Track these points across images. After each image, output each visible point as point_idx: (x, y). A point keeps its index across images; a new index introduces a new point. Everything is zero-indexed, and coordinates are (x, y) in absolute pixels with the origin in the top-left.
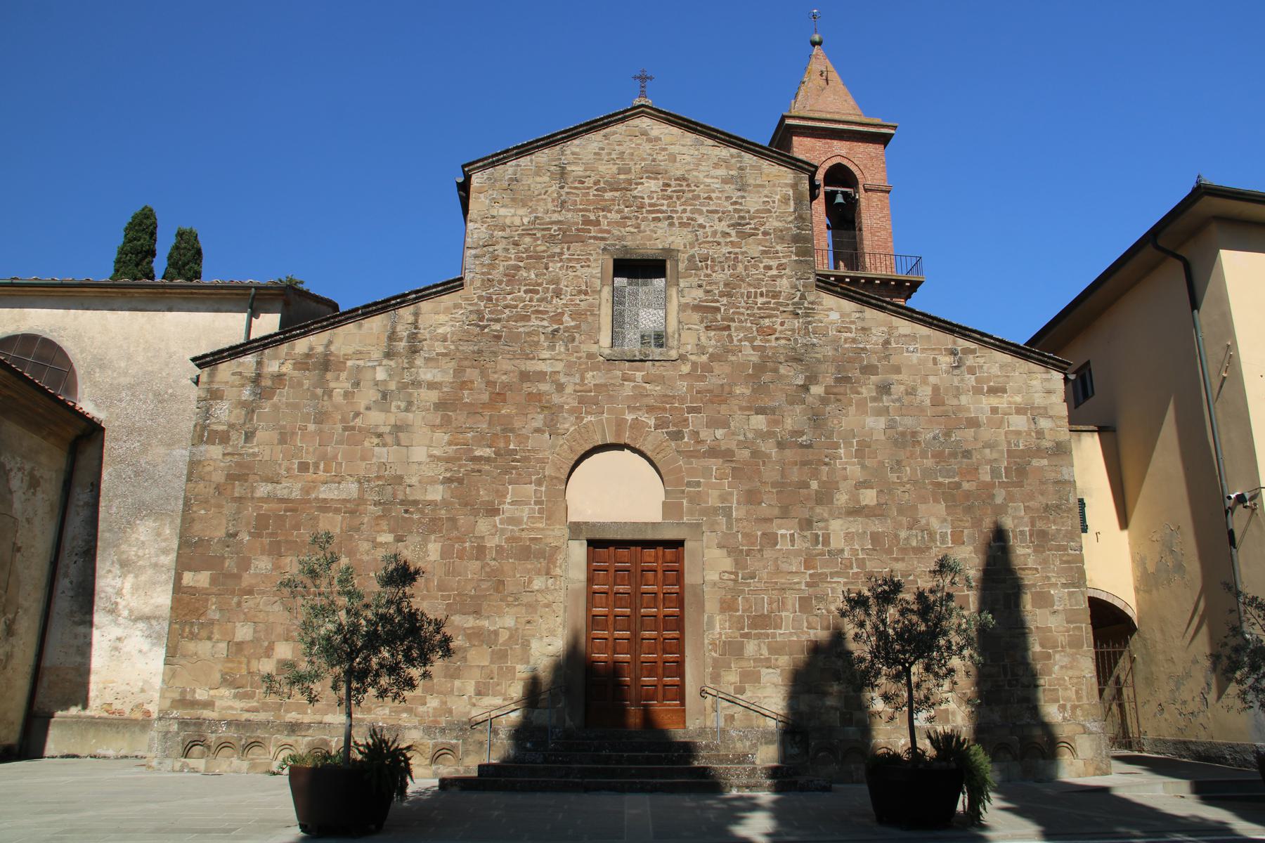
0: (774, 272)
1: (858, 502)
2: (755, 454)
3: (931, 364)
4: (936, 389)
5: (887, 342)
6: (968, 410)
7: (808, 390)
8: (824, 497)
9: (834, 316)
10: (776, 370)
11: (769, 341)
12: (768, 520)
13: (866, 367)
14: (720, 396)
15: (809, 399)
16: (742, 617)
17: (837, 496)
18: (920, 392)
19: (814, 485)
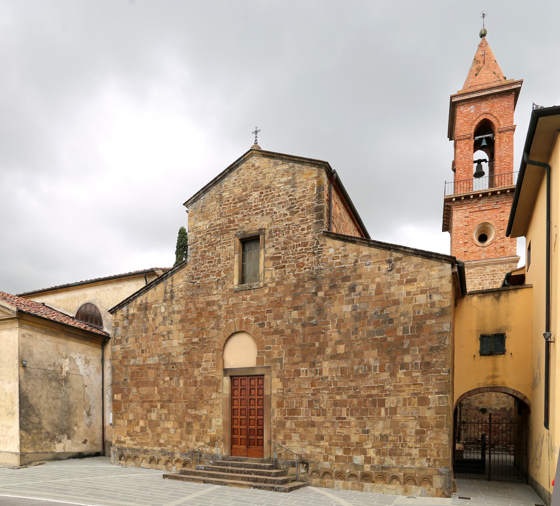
0: (306, 232)
1: (336, 352)
2: (293, 331)
3: (377, 271)
4: (378, 285)
5: (356, 261)
6: (394, 295)
7: (317, 294)
8: (321, 351)
9: (332, 251)
10: (303, 286)
11: (301, 271)
12: (297, 363)
13: (345, 277)
14: (279, 303)
15: (318, 300)
16: (285, 410)
17: (327, 349)
18: (370, 288)
19: (317, 344)
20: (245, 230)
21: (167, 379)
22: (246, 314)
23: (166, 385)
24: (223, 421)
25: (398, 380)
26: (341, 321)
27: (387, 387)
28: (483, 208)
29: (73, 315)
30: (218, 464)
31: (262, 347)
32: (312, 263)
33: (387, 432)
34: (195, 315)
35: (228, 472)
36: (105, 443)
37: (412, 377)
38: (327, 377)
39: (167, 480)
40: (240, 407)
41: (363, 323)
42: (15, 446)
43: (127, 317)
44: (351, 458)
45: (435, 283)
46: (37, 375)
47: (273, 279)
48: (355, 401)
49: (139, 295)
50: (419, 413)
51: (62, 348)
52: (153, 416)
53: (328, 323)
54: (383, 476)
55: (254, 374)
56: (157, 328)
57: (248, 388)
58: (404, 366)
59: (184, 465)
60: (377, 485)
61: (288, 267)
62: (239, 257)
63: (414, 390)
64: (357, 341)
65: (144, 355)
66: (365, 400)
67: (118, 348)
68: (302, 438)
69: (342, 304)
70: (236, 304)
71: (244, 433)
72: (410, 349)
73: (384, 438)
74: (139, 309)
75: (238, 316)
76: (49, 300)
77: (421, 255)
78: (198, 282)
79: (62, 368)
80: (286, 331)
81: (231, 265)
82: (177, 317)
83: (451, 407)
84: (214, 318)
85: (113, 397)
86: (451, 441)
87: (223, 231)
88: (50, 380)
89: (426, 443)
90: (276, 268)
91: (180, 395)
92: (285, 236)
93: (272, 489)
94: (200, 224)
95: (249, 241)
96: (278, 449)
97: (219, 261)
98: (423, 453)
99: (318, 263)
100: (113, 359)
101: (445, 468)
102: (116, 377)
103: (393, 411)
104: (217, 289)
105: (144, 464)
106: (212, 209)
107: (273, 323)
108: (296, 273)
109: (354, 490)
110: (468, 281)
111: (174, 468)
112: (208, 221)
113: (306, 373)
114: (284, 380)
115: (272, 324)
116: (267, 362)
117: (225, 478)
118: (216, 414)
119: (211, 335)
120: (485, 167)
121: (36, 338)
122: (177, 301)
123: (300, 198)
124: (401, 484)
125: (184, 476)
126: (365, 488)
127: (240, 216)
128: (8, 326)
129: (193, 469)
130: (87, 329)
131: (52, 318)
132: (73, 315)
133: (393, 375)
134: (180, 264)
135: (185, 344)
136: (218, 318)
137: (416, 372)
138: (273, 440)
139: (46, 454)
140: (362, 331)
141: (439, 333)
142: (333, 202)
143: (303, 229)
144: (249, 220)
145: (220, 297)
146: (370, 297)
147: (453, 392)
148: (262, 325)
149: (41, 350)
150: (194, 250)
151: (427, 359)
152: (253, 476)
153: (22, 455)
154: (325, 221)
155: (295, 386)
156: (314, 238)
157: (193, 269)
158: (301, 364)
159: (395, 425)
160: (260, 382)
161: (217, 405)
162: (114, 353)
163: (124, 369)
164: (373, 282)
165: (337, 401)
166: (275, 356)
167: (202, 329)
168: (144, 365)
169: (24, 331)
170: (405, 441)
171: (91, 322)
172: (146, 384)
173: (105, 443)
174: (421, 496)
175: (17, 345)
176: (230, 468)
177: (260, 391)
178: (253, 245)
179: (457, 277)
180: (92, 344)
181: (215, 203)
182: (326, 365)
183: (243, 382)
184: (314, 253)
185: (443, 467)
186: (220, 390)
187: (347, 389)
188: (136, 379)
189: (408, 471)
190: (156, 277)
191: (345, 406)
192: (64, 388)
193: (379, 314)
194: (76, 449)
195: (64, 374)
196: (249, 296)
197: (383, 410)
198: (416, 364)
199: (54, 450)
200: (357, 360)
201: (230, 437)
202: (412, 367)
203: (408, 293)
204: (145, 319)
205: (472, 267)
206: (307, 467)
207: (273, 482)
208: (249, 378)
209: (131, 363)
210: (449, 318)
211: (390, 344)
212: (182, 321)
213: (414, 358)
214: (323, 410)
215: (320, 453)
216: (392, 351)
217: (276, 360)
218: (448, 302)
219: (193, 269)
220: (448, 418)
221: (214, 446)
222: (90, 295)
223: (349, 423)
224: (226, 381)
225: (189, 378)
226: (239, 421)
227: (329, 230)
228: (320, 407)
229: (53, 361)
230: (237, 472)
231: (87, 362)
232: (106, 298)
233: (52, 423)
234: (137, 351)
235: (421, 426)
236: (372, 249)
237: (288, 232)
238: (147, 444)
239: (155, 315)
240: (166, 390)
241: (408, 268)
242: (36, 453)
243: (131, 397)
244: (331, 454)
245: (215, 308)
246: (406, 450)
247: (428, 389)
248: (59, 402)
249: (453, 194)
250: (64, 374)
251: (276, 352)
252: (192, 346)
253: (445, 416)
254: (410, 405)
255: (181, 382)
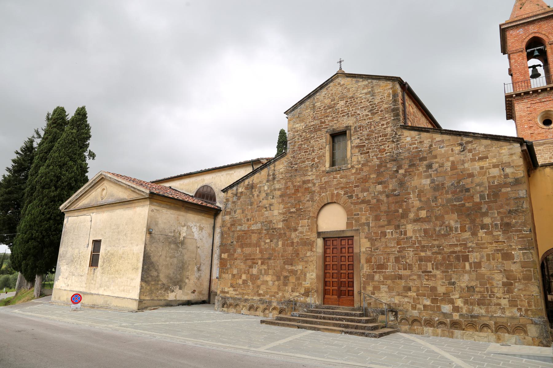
0: (385, 126)
1: (418, 216)
2: (378, 200)
3: (450, 152)
4: (453, 162)
5: (431, 146)
7: (398, 172)
8: (404, 215)
9: (409, 139)
10: (386, 166)
14: (365, 180)
15: (399, 176)
16: (373, 265)
17: (410, 214)
19: (400, 211)
20: (335, 127)
21: (268, 241)
22: (336, 189)
23: (267, 246)
24: (317, 276)
25: (480, 239)
26: (421, 192)
27: (470, 245)
28: (543, 100)
29: (193, 194)
30: (312, 312)
31: (352, 214)
32: (392, 148)
33: (473, 284)
34: (293, 191)
35: (320, 319)
36: (210, 293)
37: (493, 236)
38: (412, 237)
39: (264, 325)
40: (332, 263)
41: (442, 193)
42: (135, 294)
43: (236, 195)
44: (439, 308)
45: (506, 159)
46: (159, 240)
47: (359, 162)
48: (440, 257)
49: (247, 178)
51: (182, 219)
52: (255, 271)
53: (409, 194)
54: (473, 324)
55: (345, 235)
56: (260, 202)
57: (339, 247)
58: (483, 227)
59: (280, 312)
60: (468, 332)
61: (371, 152)
62: (330, 147)
64: (437, 207)
65: (249, 223)
66: (448, 256)
67: (227, 218)
68: (391, 289)
69: (421, 178)
70: (328, 181)
71: (335, 284)
72: (488, 212)
73: (470, 289)
74: (247, 188)
75: (330, 191)
76: (174, 185)
77: (490, 138)
78: (296, 166)
79: (180, 234)
80: (372, 201)
81: (323, 153)
82: (278, 193)
83: (537, 262)
84: (309, 193)
85: (221, 255)
86: (542, 292)
87: (316, 129)
88: (170, 243)
90: (361, 154)
91: (278, 254)
92: (368, 130)
93: (363, 334)
94: (297, 126)
95: (338, 136)
96: (368, 298)
97: (313, 151)
98: (513, 303)
99: (398, 148)
100: (223, 226)
101: (539, 318)
102: (224, 240)
103: (478, 265)
104: (312, 171)
105: (244, 311)
106: (307, 115)
107: (360, 195)
108: (379, 156)
109: (444, 336)
110: (538, 157)
111: (271, 315)
112: (304, 123)
113: (392, 234)
114: (370, 240)
115: (359, 196)
116: (356, 226)
117: (318, 324)
118: (310, 269)
119: (306, 206)
120: (541, 70)
121: (162, 212)
122: (278, 181)
123: (379, 103)
124: (492, 332)
125: (279, 322)
126: (455, 335)
127: (330, 118)
128: (141, 204)
129: (288, 316)
130: (204, 204)
131: (176, 197)
132: (193, 194)
133: (474, 234)
134: (281, 154)
135: (284, 214)
136: (312, 193)
138: (362, 291)
139: (160, 302)
140: (441, 199)
141: (516, 199)
142: (407, 104)
143: (383, 125)
144: (337, 120)
145: (314, 177)
146: (446, 172)
147: (537, 249)
148: (351, 197)
149: (165, 221)
150: (293, 144)
151: (506, 220)
152: (344, 322)
153: (140, 301)
154: (401, 118)
155: (382, 245)
156: (393, 130)
157: (291, 157)
158: (387, 227)
159: (480, 277)
160: (350, 242)
161: (311, 261)
162: (223, 221)
163: (231, 234)
164: (448, 160)
165: (422, 257)
166: (363, 220)
167: (299, 202)
168: (249, 231)
169: (153, 207)
170: (492, 292)
171: (207, 199)
172: (249, 245)
173: (210, 293)
174: (516, 344)
175: (146, 217)
176: (323, 315)
177: (350, 250)
178: (341, 138)
179: (527, 153)
180: (206, 216)
181: (309, 110)
182: (410, 227)
183: (335, 243)
184: (393, 142)
185: (537, 316)
186: (314, 249)
187: (431, 247)
188: (241, 241)
189: (498, 320)
190: (261, 165)
191: (431, 261)
192: (180, 249)
193: (456, 185)
194: (186, 298)
195: (181, 238)
196: (338, 176)
197: (467, 265)
198: (496, 225)
199: (167, 298)
200: (438, 223)
201: (323, 288)
202: (492, 227)
203: (481, 168)
204: (251, 196)
205: (540, 145)
206: (396, 315)
207: (364, 328)
208: (340, 239)
209: (238, 229)
210: (525, 186)
211: (468, 208)
212: (281, 196)
213: (493, 219)
214: (409, 265)
215: (408, 302)
216: (471, 214)
217: (364, 224)
218: (521, 173)
219: (291, 157)
220: (536, 272)
221: (308, 296)
222: (207, 180)
223: (435, 276)
224: (320, 242)
225: (287, 240)
226: (331, 274)
227: (405, 124)
228: (406, 263)
229: (173, 228)
230: (329, 319)
231: (201, 229)
232: (219, 182)
233: (168, 277)
234: (243, 219)
235: (508, 279)
236: (444, 136)
237: (370, 127)
238: (248, 294)
239: (260, 192)
240: (266, 250)
241: (480, 148)
242: (152, 300)
243: (236, 256)
244: (419, 303)
245: (310, 185)
246: (495, 300)
248: (175, 260)
249: (512, 91)
250: (181, 238)
251: (364, 217)
252: (290, 215)
254: (494, 259)
255: (280, 243)
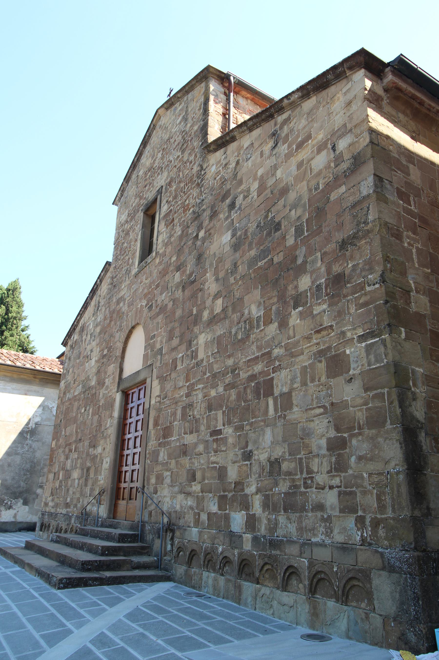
27: (276, 352)
33: (278, 452)
50: (331, 396)
58: (298, 300)
63: (318, 344)
89: (350, 472)
137: (319, 304)
151: (336, 269)
170: (310, 471)
197: (271, 402)
213: (314, 276)
235: (338, 429)
247: (343, 333)
253: (386, 390)
254: (313, 380)
